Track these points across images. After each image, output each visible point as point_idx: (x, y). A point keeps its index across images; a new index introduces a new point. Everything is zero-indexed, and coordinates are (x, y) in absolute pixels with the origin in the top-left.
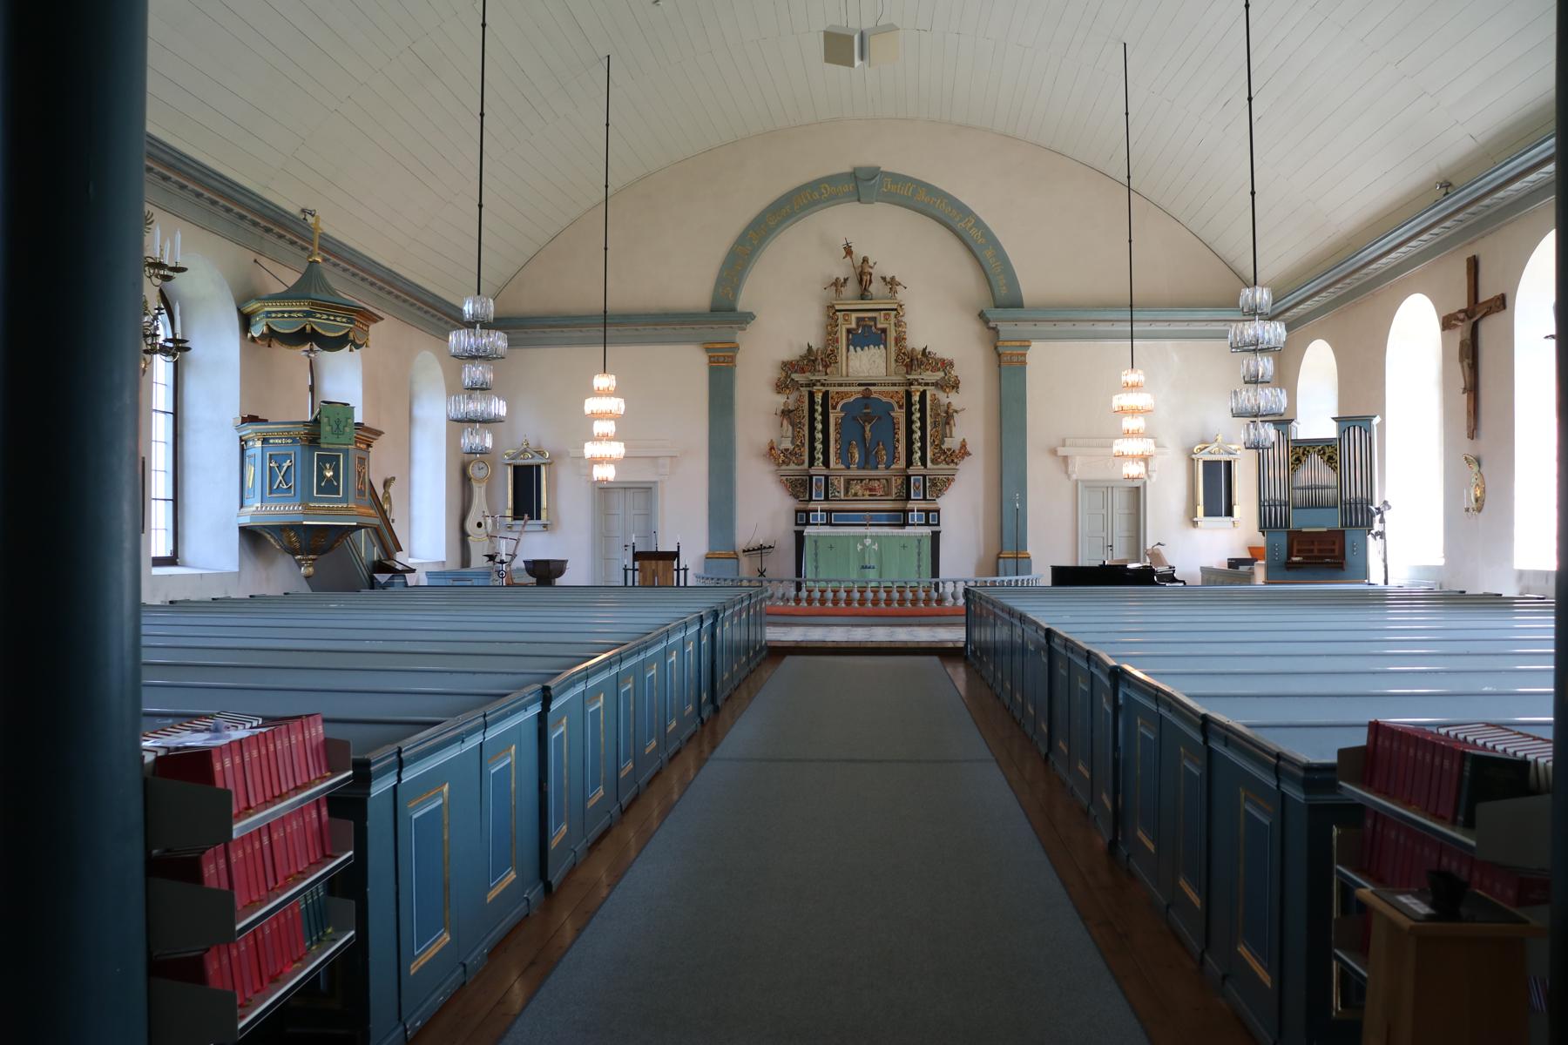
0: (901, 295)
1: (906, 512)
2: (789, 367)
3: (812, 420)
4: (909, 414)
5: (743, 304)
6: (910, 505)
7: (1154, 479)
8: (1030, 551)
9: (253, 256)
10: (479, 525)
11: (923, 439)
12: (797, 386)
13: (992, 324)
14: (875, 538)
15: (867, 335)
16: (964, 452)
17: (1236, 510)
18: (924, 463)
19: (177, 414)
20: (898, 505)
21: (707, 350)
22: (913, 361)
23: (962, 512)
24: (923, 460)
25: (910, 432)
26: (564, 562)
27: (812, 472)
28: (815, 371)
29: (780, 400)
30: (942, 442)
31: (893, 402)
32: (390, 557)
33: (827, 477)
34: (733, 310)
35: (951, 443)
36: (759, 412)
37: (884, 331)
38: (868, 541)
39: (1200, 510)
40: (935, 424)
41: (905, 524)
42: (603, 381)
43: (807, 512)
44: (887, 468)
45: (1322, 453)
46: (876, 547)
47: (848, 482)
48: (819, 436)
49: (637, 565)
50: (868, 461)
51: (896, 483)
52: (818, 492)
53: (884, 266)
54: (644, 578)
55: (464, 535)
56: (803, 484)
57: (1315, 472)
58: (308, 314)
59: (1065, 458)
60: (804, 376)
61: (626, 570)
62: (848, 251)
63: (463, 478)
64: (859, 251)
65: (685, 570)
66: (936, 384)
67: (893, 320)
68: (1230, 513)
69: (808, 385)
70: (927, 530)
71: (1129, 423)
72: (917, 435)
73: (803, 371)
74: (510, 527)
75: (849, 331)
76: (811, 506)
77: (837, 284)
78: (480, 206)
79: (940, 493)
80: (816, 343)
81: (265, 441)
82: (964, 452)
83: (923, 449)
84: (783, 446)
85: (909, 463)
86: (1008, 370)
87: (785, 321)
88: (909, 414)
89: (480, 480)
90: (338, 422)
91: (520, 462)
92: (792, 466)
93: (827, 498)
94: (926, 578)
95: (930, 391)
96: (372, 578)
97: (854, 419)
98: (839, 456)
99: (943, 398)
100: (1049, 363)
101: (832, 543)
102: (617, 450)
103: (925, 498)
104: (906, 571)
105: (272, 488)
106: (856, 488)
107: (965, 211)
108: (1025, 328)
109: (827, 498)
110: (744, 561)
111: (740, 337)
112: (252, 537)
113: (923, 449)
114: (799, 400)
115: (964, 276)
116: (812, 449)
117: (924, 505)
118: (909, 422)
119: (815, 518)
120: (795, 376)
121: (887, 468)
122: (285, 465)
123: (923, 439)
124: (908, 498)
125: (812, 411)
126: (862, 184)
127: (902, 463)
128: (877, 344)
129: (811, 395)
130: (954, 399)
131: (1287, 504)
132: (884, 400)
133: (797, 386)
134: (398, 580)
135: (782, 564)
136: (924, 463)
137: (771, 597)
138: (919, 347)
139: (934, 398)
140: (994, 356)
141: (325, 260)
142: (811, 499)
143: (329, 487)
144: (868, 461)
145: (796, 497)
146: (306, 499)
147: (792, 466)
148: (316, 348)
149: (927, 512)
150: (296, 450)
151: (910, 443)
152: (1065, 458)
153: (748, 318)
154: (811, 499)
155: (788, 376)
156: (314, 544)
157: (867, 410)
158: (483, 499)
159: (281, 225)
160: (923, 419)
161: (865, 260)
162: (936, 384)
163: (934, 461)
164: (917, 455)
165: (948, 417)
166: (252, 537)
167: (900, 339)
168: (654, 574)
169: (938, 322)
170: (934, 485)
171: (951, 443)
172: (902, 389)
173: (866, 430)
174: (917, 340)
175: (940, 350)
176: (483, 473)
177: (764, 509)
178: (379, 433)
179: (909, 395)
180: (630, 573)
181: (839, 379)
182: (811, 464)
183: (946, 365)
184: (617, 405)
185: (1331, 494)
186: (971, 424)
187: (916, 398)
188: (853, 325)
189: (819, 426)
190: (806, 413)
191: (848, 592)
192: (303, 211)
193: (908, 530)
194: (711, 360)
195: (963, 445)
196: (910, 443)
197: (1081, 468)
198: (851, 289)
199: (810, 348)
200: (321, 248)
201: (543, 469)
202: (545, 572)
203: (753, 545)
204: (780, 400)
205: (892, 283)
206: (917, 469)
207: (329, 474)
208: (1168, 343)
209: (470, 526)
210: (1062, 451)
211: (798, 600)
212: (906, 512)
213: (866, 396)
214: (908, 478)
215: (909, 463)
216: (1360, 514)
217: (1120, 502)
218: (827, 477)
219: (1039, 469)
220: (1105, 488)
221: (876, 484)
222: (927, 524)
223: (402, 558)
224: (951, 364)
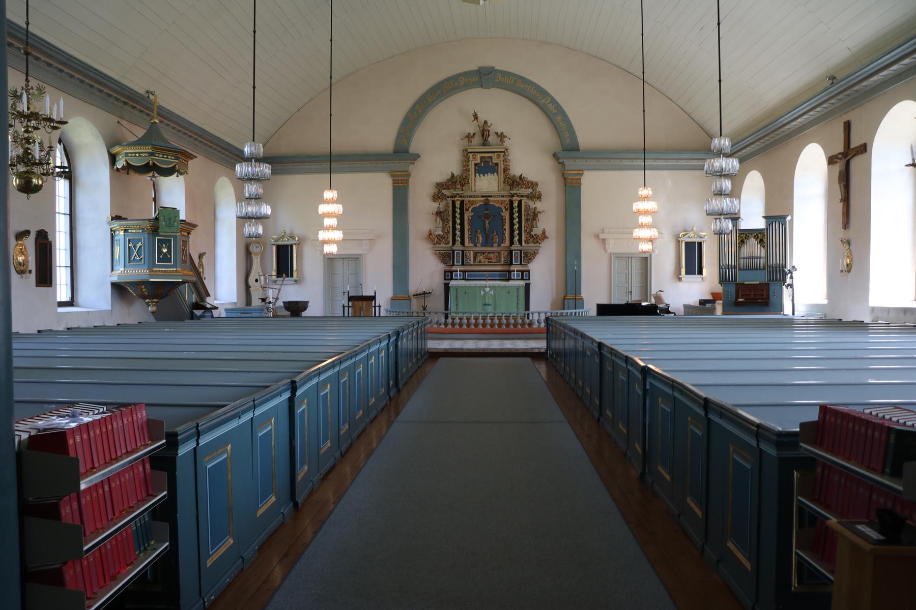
0: (507, 143)
1: (510, 272)
3: (454, 217)
4: (512, 214)
5: (413, 149)
6: (512, 268)
7: (656, 252)
8: (583, 294)
9: (117, 119)
10: (257, 281)
11: (520, 228)
12: (445, 197)
13: (561, 161)
14: (491, 287)
15: (486, 167)
16: (544, 236)
17: (704, 271)
18: (520, 243)
19: (72, 215)
21: (392, 176)
23: (543, 272)
24: (520, 241)
25: (512, 225)
26: (307, 302)
27: (454, 248)
28: (455, 189)
30: (531, 231)
32: (203, 300)
34: (407, 152)
35: (537, 231)
36: (423, 213)
37: (497, 164)
38: (488, 289)
39: (683, 270)
40: (527, 220)
41: (509, 279)
42: (329, 194)
43: (451, 272)
44: (499, 246)
45: (756, 237)
47: (475, 254)
48: (458, 227)
49: (350, 304)
50: (487, 242)
51: (504, 255)
52: (457, 261)
53: (497, 126)
54: (355, 312)
55: (248, 286)
56: (449, 255)
57: (753, 249)
58: (152, 154)
60: (450, 191)
61: (344, 307)
62: (476, 117)
63: (247, 252)
64: (482, 117)
65: (379, 306)
67: (502, 158)
68: (700, 273)
69: (451, 197)
70: (522, 283)
71: (643, 219)
72: (516, 226)
74: (275, 282)
75: (476, 165)
76: (454, 268)
77: (469, 137)
78: (254, 88)
81: (126, 231)
82: (544, 236)
83: (520, 235)
84: (437, 233)
85: (512, 243)
86: (571, 189)
87: (439, 160)
88: (512, 214)
89: (257, 254)
90: (170, 219)
91: (280, 243)
92: (442, 245)
93: (463, 264)
94: (522, 311)
96: (192, 313)
97: (479, 217)
99: (532, 204)
100: (595, 184)
102: (338, 235)
103: (521, 264)
104: (509, 307)
105: (130, 259)
106: (481, 258)
107: (545, 93)
108: (580, 163)
109: (463, 264)
110: (414, 301)
111: (411, 168)
112: (119, 289)
113: (520, 235)
114: (447, 205)
116: (454, 235)
117: (520, 268)
118: (512, 219)
119: (456, 275)
120: (444, 192)
121: (499, 246)
122: (138, 246)
123: (520, 228)
124: (511, 264)
125: (454, 212)
126: (485, 77)
127: (508, 243)
128: (492, 173)
129: (454, 202)
130: (539, 205)
131: (735, 267)
132: (497, 205)
133: (445, 197)
134: (207, 314)
136: (520, 243)
137: (431, 322)
138: (518, 174)
139: (526, 205)
140: (562, 179)
141: (161, 122)
142: (453, 264)
143: (165, 258)
144: (487, 242)
145: (444, 262)
146: (151, 265)
147: (442, 245)
148: (156, 174)
149: (522, 272)
150: (144, 237)
152: (604, 240)
153: (416, 157)
154: (453, 264)
155: (439, 191)
156: (158, 293)
158: (259, 265)
159: (133, 100)
160: (520, 217)
161: (486, 122)
163: (526, 242)
164: (516, 239)
165: (534, 216)
166: (119, 289)
167: (506, 170)
168: (361, 309)
169: (530, 160)
170: (526, 256)
171: (537, 231)
172: (507, 199)
173: (486, 224)
175: (530, 176)
177: (426, 271)
178: (195, 226)
179: (511, 202)
180: (346, 309)
181: (470, 193)
182: (454, 243)
183: (533, 185)
184: (337, 208)
185: (761, 262)
186: (549, 219)
187: (516, 204)
188: (479, 161)
189: (458, 221)
190: (451, 213)
191: (476, 319)
192: (147, 92)
193: (511, 283)
194: (394, 182)
195: (544, 232)
197: (612, 247)
198: (477, 139)
199: (453, 175)
200: (158, 114)
201: (294, 247)
202: (296, 309)
203: (420, 291)
204: (435, 206)
205: (501, 136)
206: (516, 246)
207: (165, 251)
208: (665, 173)
209: (251, 281)
210: (602, 236)
211: (446, 324)
212: (510, 272)
213: (486, 203)
214: (511, 252)
215: (512, 243)
216: (779, 274)
217: (636, 266)
218: (463, 251)
219: (588, 246)
220: (627, 258)
221: (492, 255)
222: (522, 279)
223: (210, 301)
224: (537, 184)
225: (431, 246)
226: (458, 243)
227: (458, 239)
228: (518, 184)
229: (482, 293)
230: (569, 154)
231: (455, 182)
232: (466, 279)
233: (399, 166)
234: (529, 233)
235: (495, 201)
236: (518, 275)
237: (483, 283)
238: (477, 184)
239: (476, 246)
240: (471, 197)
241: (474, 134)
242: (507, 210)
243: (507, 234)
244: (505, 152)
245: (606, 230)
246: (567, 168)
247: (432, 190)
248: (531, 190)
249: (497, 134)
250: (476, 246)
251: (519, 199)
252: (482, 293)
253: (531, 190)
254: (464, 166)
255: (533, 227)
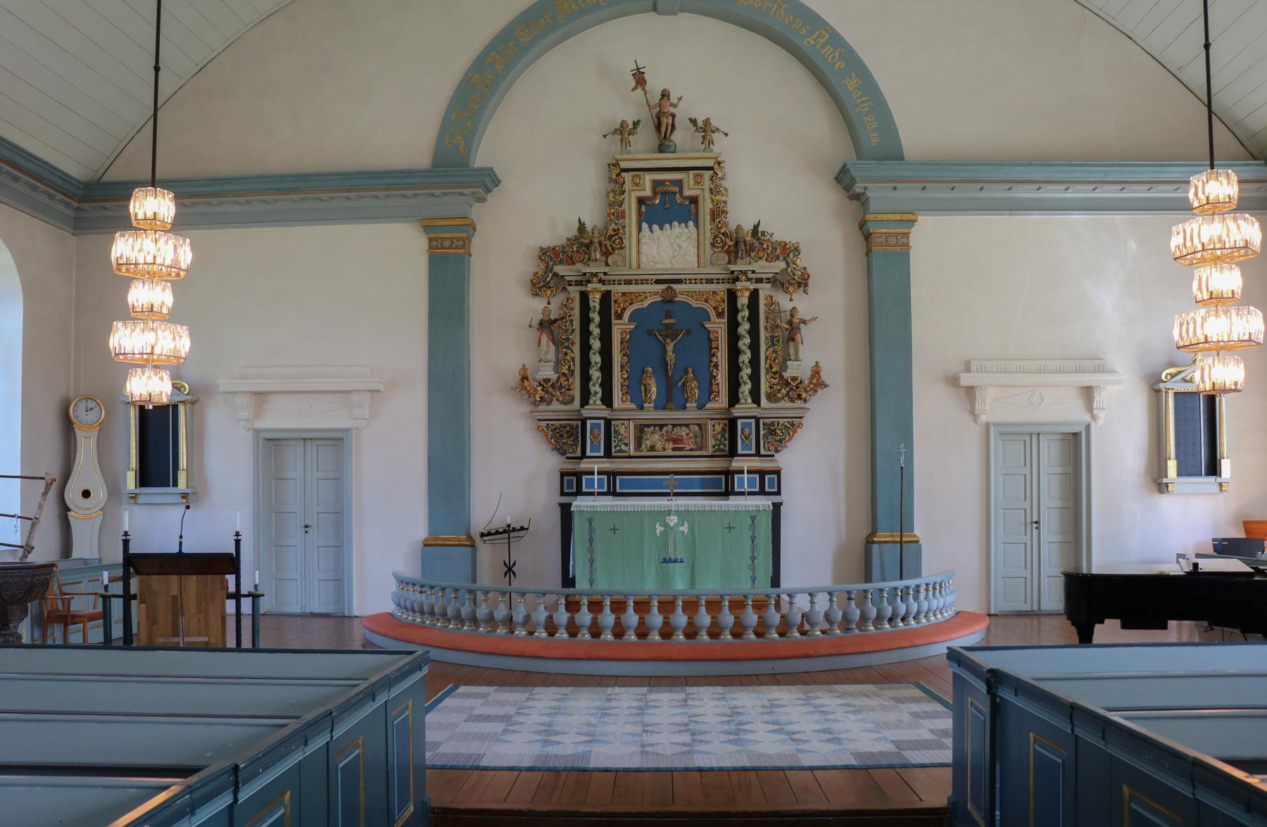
0: (720, 146)
1: (729, 474)
2: (549, 255)
3: (585, 334)
4: (733, 325)
6: (736, 464)
7: (1101, 422)
8: (918, 531)
10: (86, 494)
11: (755, 363)
12: (562, 283)
13: (858, 188)
14: (684, 515)
15: (668, 206)
16: (817, 382)
17: (1226, 466)
18: (756, 400)
20: (718, 464)
21: (427, 228)
22: (739, 245)
23: (815, 470)
24: (755, 395)
25: (734, 352)
27: (586, 413)
29: (536, 307)
30: (784, 367)
31: (708, 307)
33: (608, 422)
34: (468, 166)
35: (798, 369)
36: (507, 327)
37: (694, 200)
39: (1172, 465)
40: (772, 341)
41: (728, 493)
43: (578, 475)
44: (701, 407)
46: (685, 528)
47: (641, 430)
48: (596, 358)
50: (669, 399)
51: (715, 430)
53: (689, 106)
56: (571, 432)
59: (970, 392)
62: (640, 79)
64: (655, 84)
66: (773, 281)
67: (707, 184)
69: (579, 283)
70: (765, 502)
72: (745, 357)
73: (571, 261)
74: (134, 497)
75: (641, 201)
76: (585, 465)
79: (779, 445)
80: (593, 219)
82: (817, 382)
83: (755, 378)
85: (734, 399)
88: (733, 325)
92: (556, 406)
93: (608, 454)
95: (765, 290)
97: (650, 333)
98: (628, 391)
99: (784, 302)
100: (946, 250)
101: (616, 523)
103: (758, 454)
106: (653, 438)
108: (908, 194)
109: (608, 454)
110: (485, 551)
113: (755, 378)
115: (810, 118)
116: (586, 379)
117: (757, 463)
118: (733, 338)
120: (561, 269)
121: (701, 407)
123: (755, 363)
124: (733, 453)
125: (585, 320)
127: (722, 400)
128: (683, 220)
129: (584, 297)
132: (695, 304)
133: (562, 283)
135: (538, 559)
136: (756, 400)
139: (771, 302)
142: (584, 456)
144: (669, 399)
147: (556, 406)
149: (762, 473)
151: (734, 369)
152: (970, 392)
153: (487, 181)
154: (584, 456)
155: (548, 269)
157: (669, 318)
160: (754, 333)
162: (773, 281)
163: (771, 397)
164: (746, 388)
165: (792, 330)
167: (718, 213)
169: (775, 187)
170: (772, 432)
171: (798, 369)
172: (722, 288)
173: (668, 355)
174: (742, 216)
175: (779, 229)
176: (92, 416)
177: (513, 472)
179: (732, 296)
181: (624, 272)
182: (585, 401)
183: (787, 251)
187: (743, 300)
188: (648, 192)
189: (596, 344)
190: (577, 325)
193: (734, 502)
194: (434, 244)
195: (816, 373)
196: (734, 369)
197: (992, 408)
198: (644, 138)
199: (582, 227)
201: (181, 409)
203: (498, 524)
204: (536, 307)
206: (746, 407)
208: (1119, 218)
209: (73, 495)
210: (966, 379)
212: (729, 474)
214: (732, 422)
215: (734, 399)
217: (1050, 457)
218: (608, 422)
219: (931, 407)
220: (1030, 435)
221: (683, 432)
222: (762, 492)
224: (797, 250)
225: (529, 408)
226: (596, 400)
227: (596, 388)
228: (750, 249)
229: (659, 529)
230: (874, 176)
231: (588, 246)
232: (615, 494)
233: (446, 205)
234: (778, 374)
235: (688, 293)
236: (751, 484)
237: (661, 503)
238: (644, 249)
239: (641, 408)
240: (629, 282)
241: (636, 124)
242: (720, 315)
243: (722, 377)
244: (714, 169)
245: (974, 366)
246: (873, 206)
247: (528, 266)
248: (782, 265)
249: (693, 122)
250: (641, 408)
251: (753, 286)
252: (659, 529)
253: (781, 265)
254: (611, 205)
255: (787, 358)
